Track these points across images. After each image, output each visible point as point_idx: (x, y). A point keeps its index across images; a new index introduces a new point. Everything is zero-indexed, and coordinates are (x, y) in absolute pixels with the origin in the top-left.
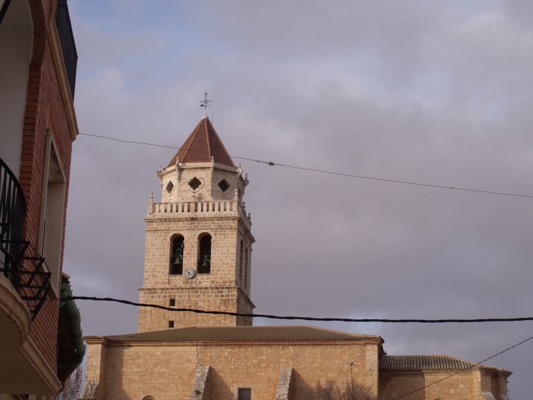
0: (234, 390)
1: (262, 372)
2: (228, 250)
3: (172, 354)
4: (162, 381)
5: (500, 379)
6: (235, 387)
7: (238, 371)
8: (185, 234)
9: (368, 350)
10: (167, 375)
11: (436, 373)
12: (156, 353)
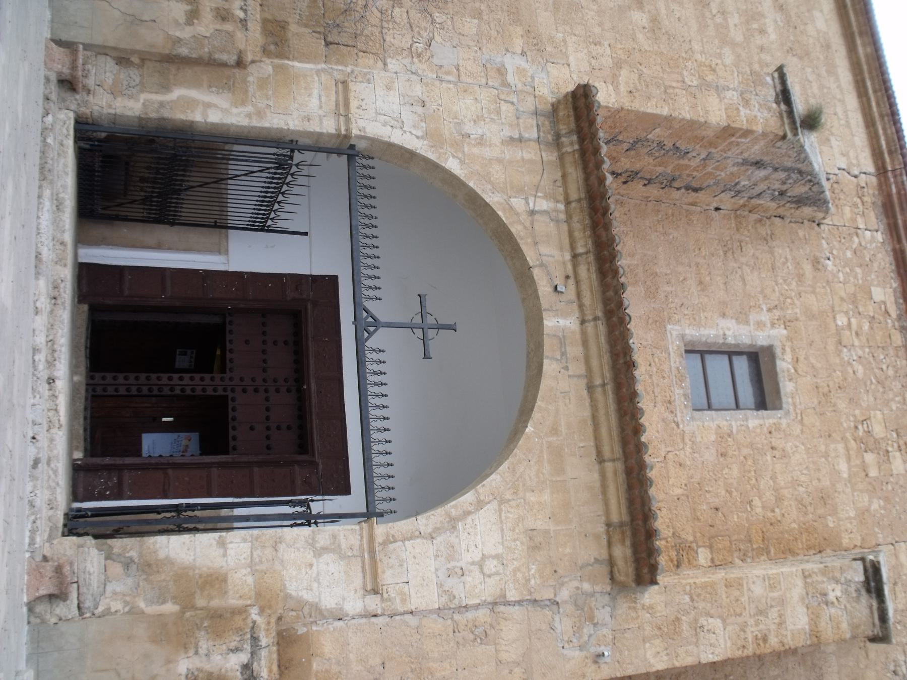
0: (760, 325)
1: (849, 460)
3: (829, 72)
4: (734, 19)
6: (773, 332)
7: (831, 347)
10: (759, 42)
12: (817, 14)
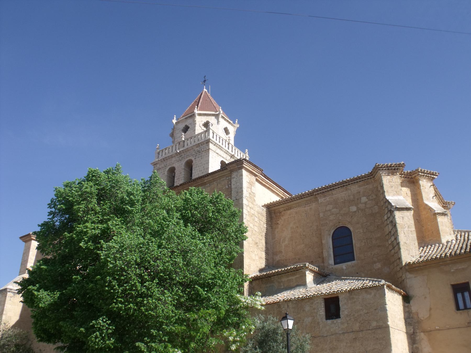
2: (204, 167)
5: (421, 182)
8: (176, 165)
9: (234, 178)
11: (330, 192)
